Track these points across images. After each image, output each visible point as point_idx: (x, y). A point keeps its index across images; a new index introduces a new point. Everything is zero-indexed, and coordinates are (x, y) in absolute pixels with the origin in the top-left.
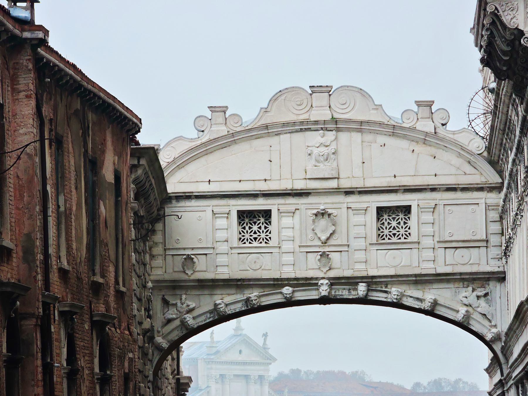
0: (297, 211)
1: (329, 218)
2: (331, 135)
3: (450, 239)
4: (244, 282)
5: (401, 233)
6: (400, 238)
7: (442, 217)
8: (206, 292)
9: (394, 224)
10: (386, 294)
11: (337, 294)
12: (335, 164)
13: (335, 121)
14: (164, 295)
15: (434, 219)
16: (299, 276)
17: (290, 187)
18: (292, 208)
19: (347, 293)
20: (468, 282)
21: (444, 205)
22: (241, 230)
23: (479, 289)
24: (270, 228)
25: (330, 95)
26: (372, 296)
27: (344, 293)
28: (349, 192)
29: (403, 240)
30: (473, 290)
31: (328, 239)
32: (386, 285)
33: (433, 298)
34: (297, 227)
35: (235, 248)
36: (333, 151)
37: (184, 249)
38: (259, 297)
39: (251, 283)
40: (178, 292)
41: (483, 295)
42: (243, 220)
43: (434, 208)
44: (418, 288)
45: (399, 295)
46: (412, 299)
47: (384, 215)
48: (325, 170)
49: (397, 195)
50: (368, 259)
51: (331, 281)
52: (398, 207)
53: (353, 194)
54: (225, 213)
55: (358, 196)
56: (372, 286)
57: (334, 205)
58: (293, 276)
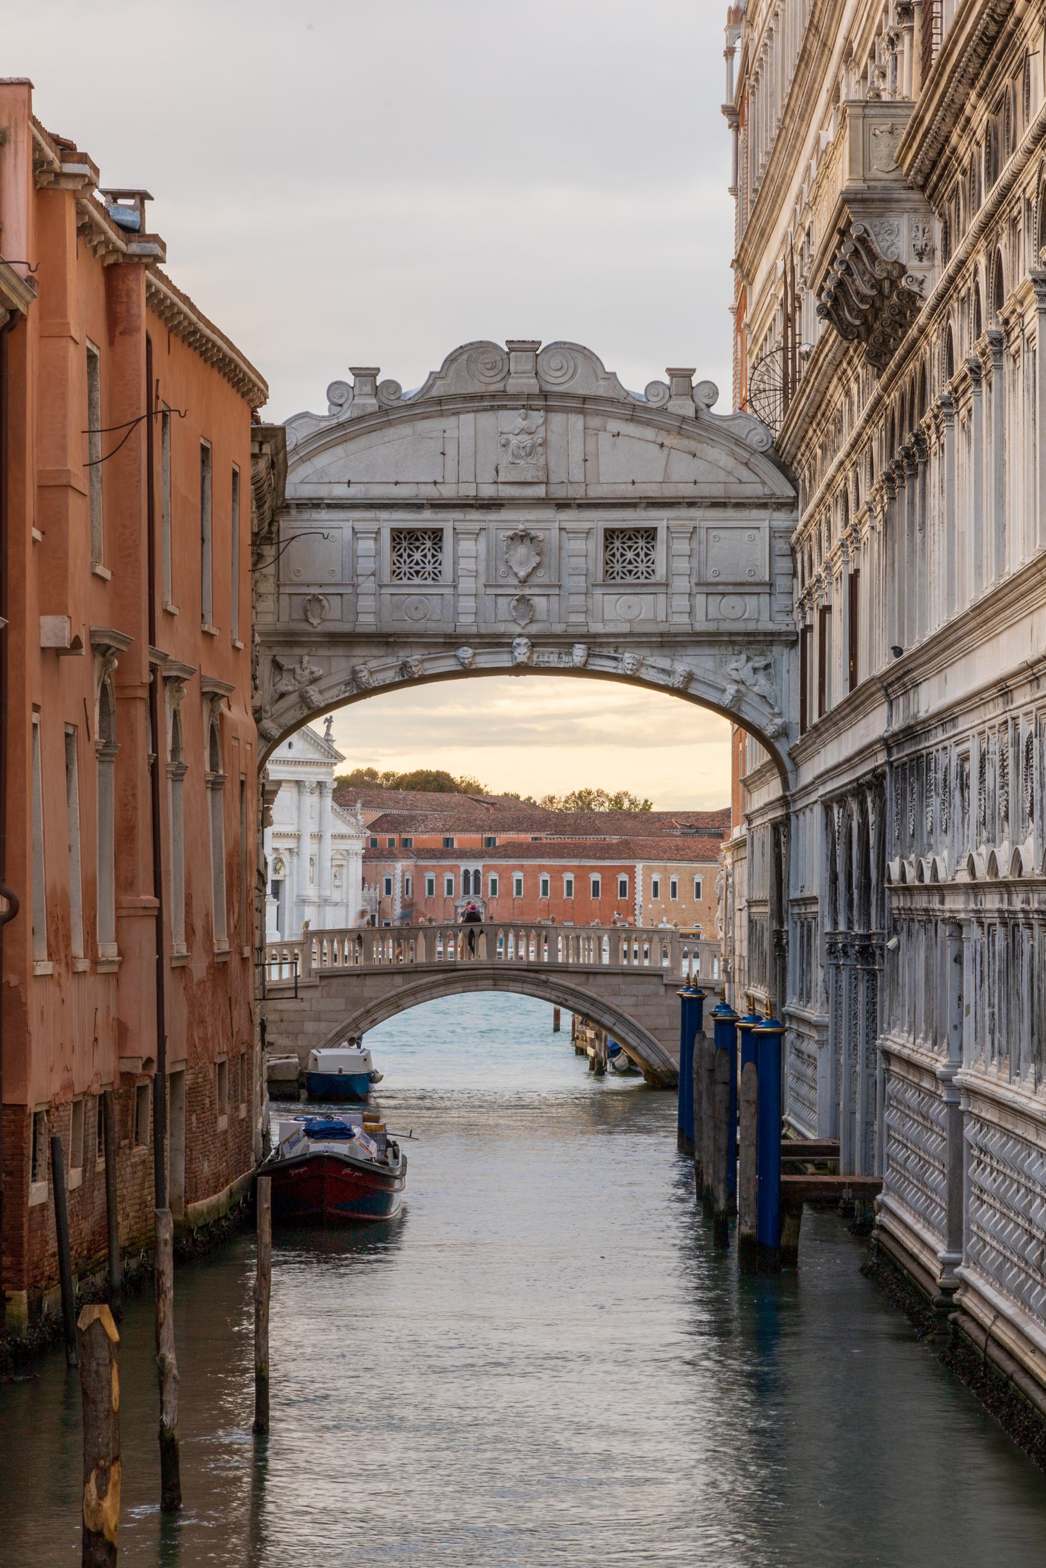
0: (483, 532)
2: (537, 417)
3: (715, 580)
6: (638, 578)
7: (703, 547)
8: (341, 651)
9: (630, 555)
12: (542, 461)
13: (545, 395)
16: (483, 631)
17: (473, 493)
18: (476, 526)
19: (556, 660)
22: (395, 558)
23: (757, 658)
24: (440, 556)
25: (537, 355)
27: (551, 659)
28: (562, 505)
29: (642, 580)
30: (749, 659)
31: (529, 575)
33: (688, 669)
34: (483, 556)
35: (386, 586)
36: (539, 441)
37: (308, 586)
38: (422, 662)
39: (410, 640)
40: (297, 651)
42: (399, 543)
43: (692, 533)
47: (615, 541)
48: (527, 471)
50: (590, 607)
52: (637, 530)
58: (474, 630)
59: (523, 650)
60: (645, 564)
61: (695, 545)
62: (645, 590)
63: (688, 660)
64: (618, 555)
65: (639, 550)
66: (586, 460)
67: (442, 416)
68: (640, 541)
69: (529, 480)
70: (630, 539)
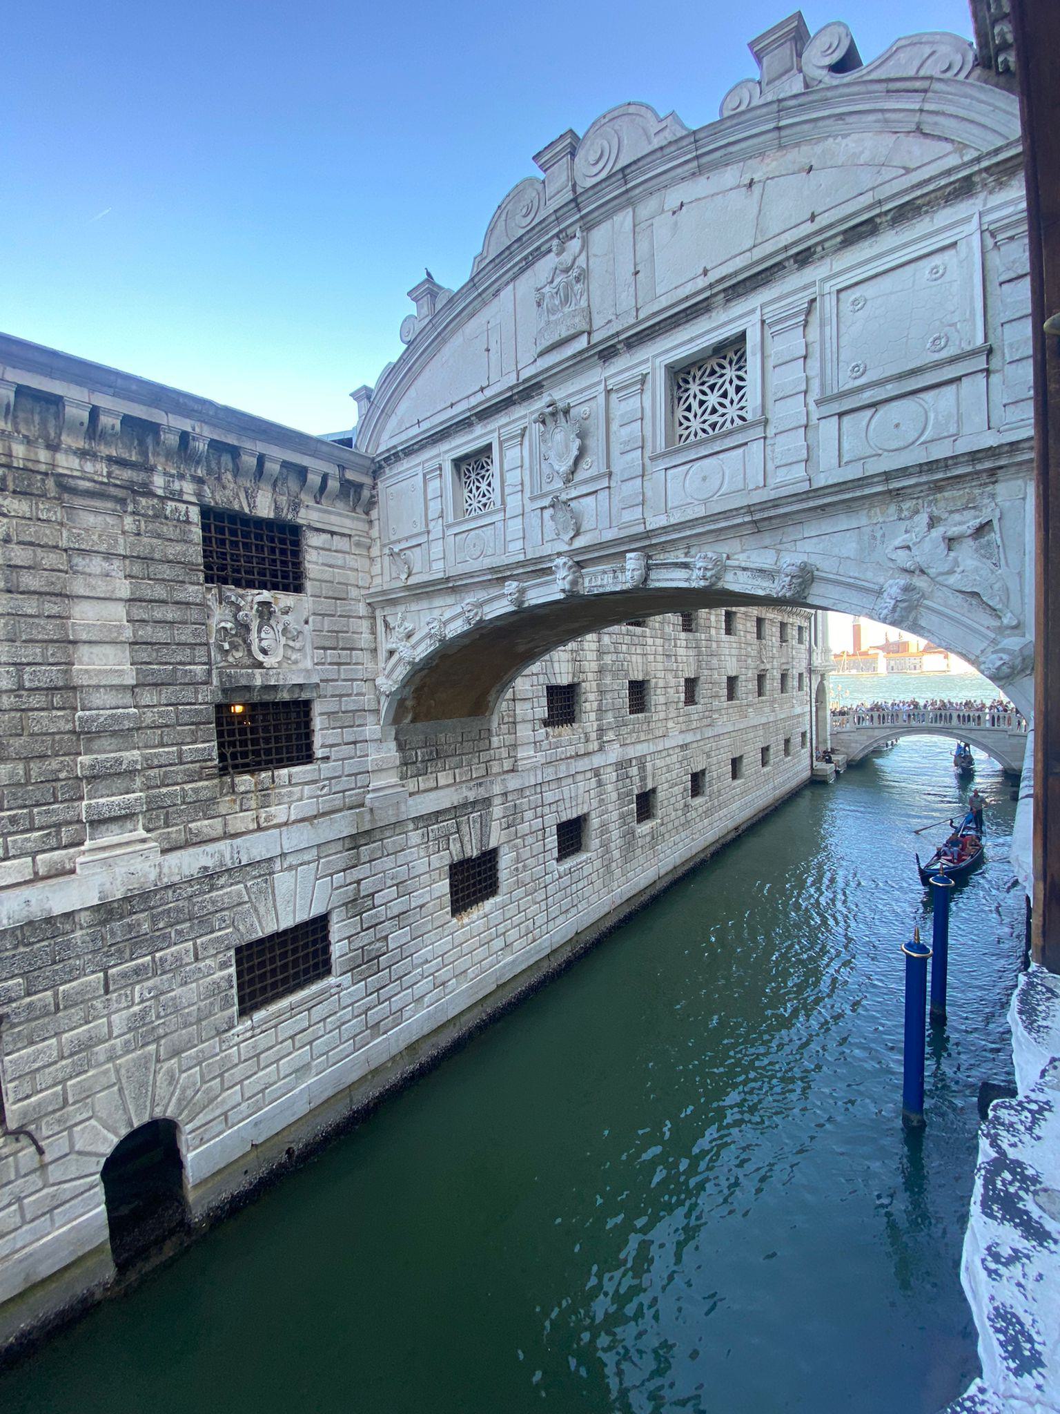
5: (728, 417)
7: (830, 331)
9: (713, 399)
12: (583, 303)
15: (806, 346)
18: (516, 428)
20: (914, 502)
21: (839, 291)
23: (957, 517)
26: (659, 580)
27: (605, 582)
28: (607, 353)
30: (933, 522)
41: (970, 532)
44: (766, 544)
49: (710, 317)
54: (435, 470)
56: (657, 557)
57: (584, 394)
59: (562, 573)
60: (736, 406)
61: (814, 333)
62: (728, 443)
63: (808, 546)
64: (695, 405)
65: (727, 385)
66: (637, 273)
67: (485, 304)
69: (564, 335)
70: (713, 372)
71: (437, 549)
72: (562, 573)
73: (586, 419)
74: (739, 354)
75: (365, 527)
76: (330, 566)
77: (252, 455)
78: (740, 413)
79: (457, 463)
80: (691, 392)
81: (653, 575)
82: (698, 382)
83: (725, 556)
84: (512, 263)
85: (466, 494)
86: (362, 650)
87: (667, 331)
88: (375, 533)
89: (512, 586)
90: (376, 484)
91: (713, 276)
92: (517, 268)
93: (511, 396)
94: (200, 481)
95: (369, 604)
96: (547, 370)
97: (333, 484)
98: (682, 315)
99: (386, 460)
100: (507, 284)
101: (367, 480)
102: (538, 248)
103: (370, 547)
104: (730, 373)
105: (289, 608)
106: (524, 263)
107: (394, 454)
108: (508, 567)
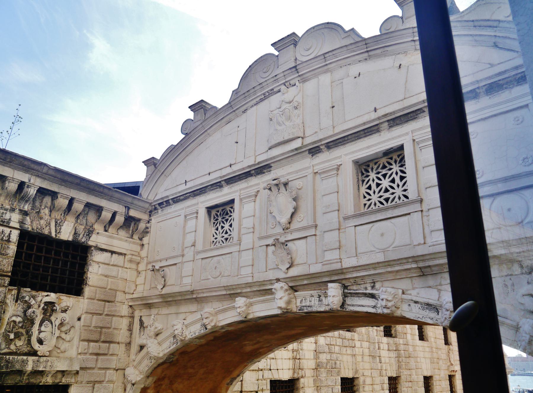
1: (286, 190)
4: (198, 293)
9: (385, 183)
10: (374, 300)
11: (304, 304)
12: (299, 121)
14: (141, 317)
18: (253, 191)
19: (317, 303)
26: (353, 305)
27: (312, 303)
28: (314, 151)
32: (372, 284)
45: (390, 299)
46: (419, 306)
51: (290, 285)
53: (320, 152)
55: (328, 153)
56: (351, 287)
57: (299, 173)
62: (397, 212)
64: (374, 186)
65: (394, 175)
66: (333, 107)
68: (394, 166)
69: (286, 138)
70: (384, 167)
71: (188, 268)
72: (280, 294)
73: (300, 189)
74: (400, 157)
75: (138, 248)
76: (106, 276)
77: (66, 198)
78: (404, 193)
79: (209, 210)
80: (371, 178)
81: (349, 301)
82: (375, 172)
83: (400, 291)
84: (255, 96)
85: (213, 230)
86: (118, 343)
87: (353, 141)
88: (144, 253)
89: (240, 302)
90: (151, 220)
91: (380, 113)
92: (259, 99)
93: (250, 171)
94: (25, 213)
95: (131, 306)
96: (274, 158)
97: (120, 219)
98: (362, 133)
99: (160, 204)
100: (252, 106)
101: (144, 217)
102: (272, 89)
103: (138, 263)
104: (396, 168)
105: (68, 307)
106: (263, 96)
107: (166, 201)
108: (239, 286)
